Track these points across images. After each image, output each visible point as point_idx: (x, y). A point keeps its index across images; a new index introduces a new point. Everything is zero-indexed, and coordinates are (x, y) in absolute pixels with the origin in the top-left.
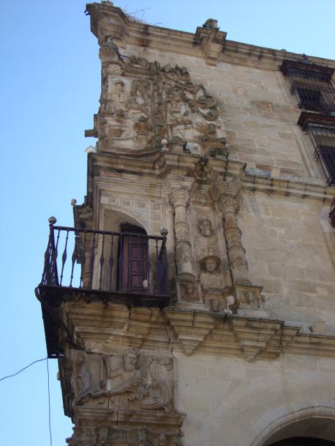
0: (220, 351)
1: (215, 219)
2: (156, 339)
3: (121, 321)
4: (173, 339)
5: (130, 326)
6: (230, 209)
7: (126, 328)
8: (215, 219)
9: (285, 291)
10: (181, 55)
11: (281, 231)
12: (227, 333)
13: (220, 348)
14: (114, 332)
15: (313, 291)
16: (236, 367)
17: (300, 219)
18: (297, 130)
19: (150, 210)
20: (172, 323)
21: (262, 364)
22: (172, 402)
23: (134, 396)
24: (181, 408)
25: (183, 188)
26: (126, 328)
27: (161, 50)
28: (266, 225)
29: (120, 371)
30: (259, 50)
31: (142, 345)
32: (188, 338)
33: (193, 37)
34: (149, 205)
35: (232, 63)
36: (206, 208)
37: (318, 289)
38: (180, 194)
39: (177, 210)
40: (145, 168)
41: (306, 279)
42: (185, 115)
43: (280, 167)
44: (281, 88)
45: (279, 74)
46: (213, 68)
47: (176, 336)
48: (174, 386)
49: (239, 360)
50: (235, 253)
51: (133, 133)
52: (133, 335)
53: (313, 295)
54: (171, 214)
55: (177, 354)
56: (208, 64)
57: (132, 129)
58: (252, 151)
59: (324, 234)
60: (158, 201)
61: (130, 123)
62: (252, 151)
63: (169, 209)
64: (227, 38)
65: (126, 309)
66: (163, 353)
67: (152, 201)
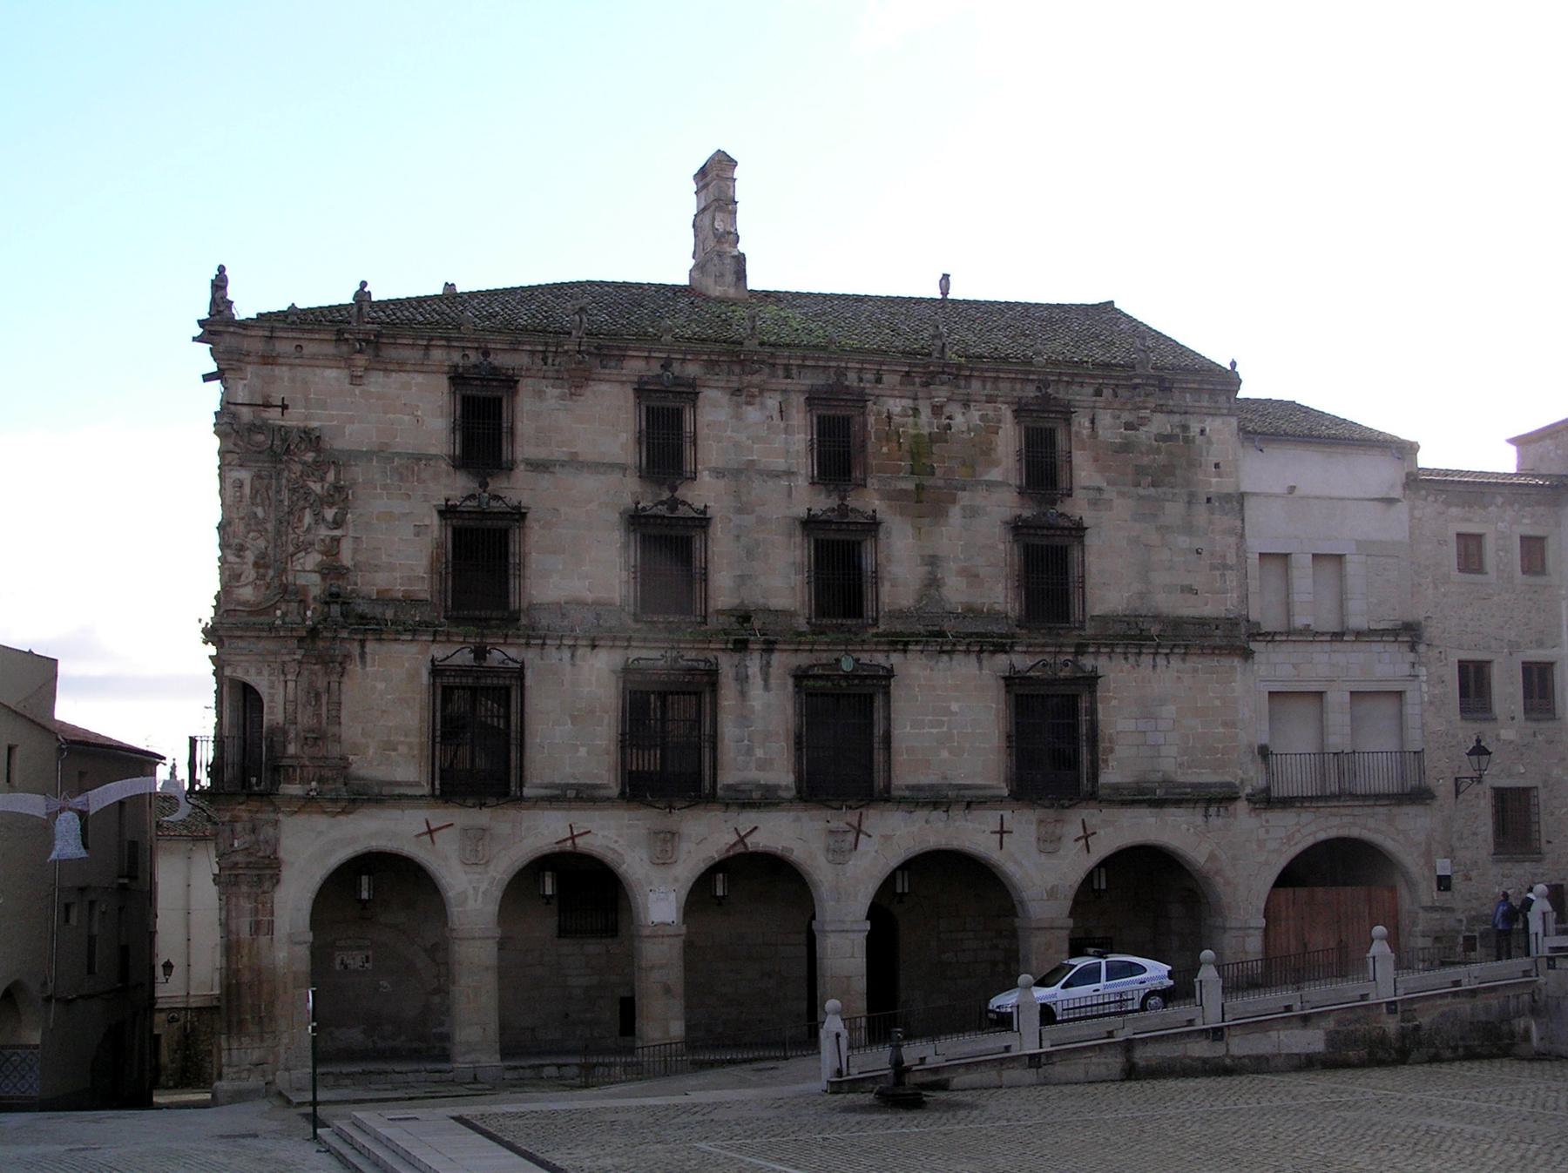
0: (310, 813)
4: (277, 810)
6: (335, 678)
8: (321, 684)
9: (371, 751)
10: (318, 371)
11: (381, 686)
15: (395, 750)
16: (321, 822)
18: (434, 520)
21: (341, 818)
22: (275, 852)
24: (282, 854)
34: (266, 673)
35: (385, 370)
37: (400, 748)
42: (308, 530)
48: (277, 840)
50: (334, 729)
55: (281, 817)
58: (377, 568)
61: (250, 556)
62: (377, 568)
66: (272, 816)
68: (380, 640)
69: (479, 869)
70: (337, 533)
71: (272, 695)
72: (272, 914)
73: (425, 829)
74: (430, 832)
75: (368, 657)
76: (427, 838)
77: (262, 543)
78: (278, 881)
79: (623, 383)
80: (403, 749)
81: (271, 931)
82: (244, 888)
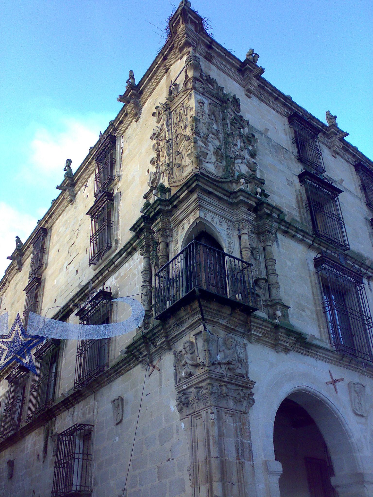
1: (261, 246)
2: (239, 330)
3: (225, 315)
5: (229, 320)
7: (227, 320)
10: (229, 78)
11: (289, 263)
12: (273, 334)
13: (266, 342)
14: (220, 322)
17: (298, 256)
18: (296, 181)
19: (225, 229)
20: (252, 324)
23: (232, 366)
24: (251, 377)
25: (248, 221)
26: (227, 320)
27: (218, 68)
28: (282, 257)
29: (224, 348)
30: (278, 93)
31: (231, 332)
32: (256, 333)
33: (240, 64)
34: (225, 225)
36: (253, 235)
38: (246, 224)
39: (243, 237)
40: (225, 195)
41: (301, 302)
43: (287, 210)
44: (286, 135)
45: (286, 120)
46: (249, 100)
47: (250, 330)
49: (272, 350)
51: (213, 159)
52: (229, 325)
53: (304, 313)
54: (237, 238)
56: (247, 95)
57: (212, 154)
59: (309, 271)
60: (230, 223)
61: (211, 148)
63: (237, 233)
64: (262, 75)
65: (230, 310)
67: (226, 222)
68: (286, 233)
69: (363, 420)
70: (253, 160)
71: (230, 243)
72: (250, 439)
73: (330, 380)
74: (334, 382)
75: (280, 242)
76: (332, 386)
77: (217, 143)
78: (254, 401)
79: (347, 161)
80: (308, 312)
81: (251, 458)
82: (231, 405)
